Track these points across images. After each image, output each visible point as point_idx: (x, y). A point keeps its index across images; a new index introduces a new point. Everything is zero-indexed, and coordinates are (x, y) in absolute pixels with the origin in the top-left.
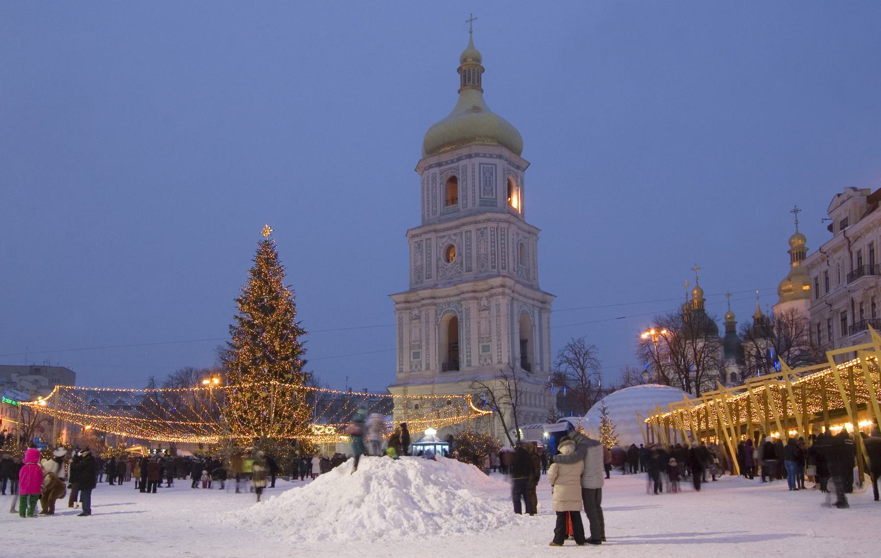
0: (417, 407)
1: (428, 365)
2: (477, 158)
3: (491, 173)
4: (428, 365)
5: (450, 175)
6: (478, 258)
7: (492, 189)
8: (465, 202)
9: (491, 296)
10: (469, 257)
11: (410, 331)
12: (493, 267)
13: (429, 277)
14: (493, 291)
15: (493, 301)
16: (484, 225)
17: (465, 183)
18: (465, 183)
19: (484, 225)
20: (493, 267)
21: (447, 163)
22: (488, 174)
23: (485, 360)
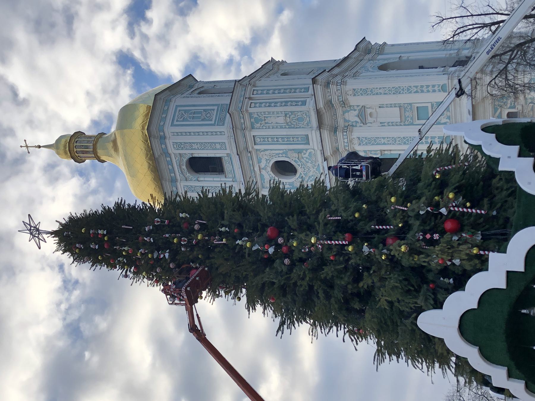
2: (166, 130)
3: (185, 111)
6: (290, 126)
7: (204, 110)
8: (218, 146)
9: (344, 103)
10: (288, 140)
12: (304, 103)
14: (335, 100)
15: (353, 101)
16: (247, 116)
17: (195, 146)
18: (195, 146)
19: (247, 116)
20: (304, 103)
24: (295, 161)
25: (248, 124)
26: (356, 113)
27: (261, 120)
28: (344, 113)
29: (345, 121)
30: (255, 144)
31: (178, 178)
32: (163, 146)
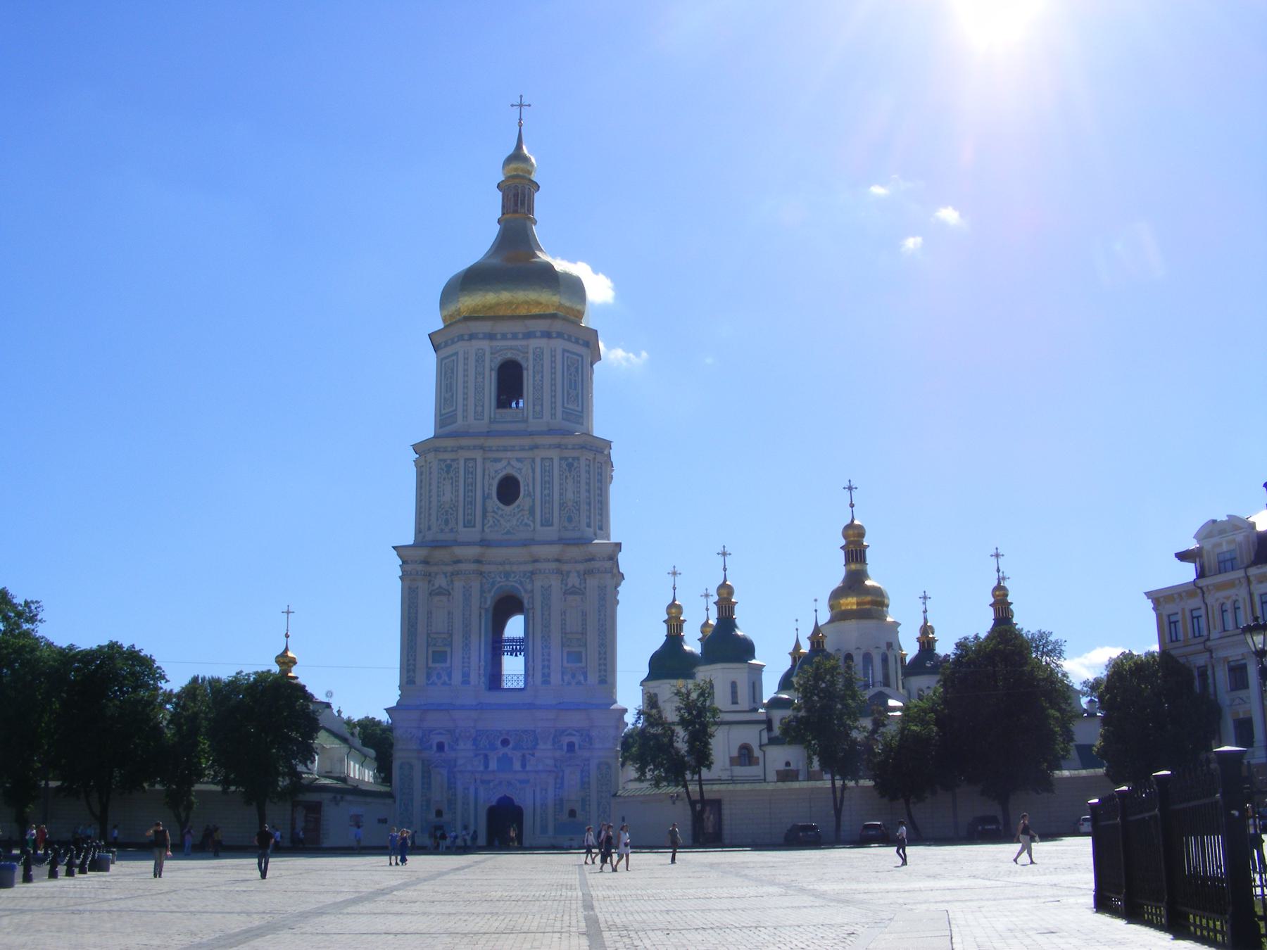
0: (441, 747)
1: (466, 675)
3: (577, 369)
4: (466, 675)
5: (509, 355)
6: (562, 505)
8: (538, 408)
9: (590, 572)
11: (430, 613)
13: (469, 524)
14: (597, 564)
15: (592, 582)
17: (538, 377)
19: (575, 454)
20: (589, 526)
21: (504, 337)
22: (573, 369)
23: (573, 676)
24: (518, 506)
25: (567, 453)
26: (577, 584)
27: (570, 471)
28: (578, 572)
29: (568, 573)
30: (542, 459)
31: (495, 343)
32: (538, 334)
